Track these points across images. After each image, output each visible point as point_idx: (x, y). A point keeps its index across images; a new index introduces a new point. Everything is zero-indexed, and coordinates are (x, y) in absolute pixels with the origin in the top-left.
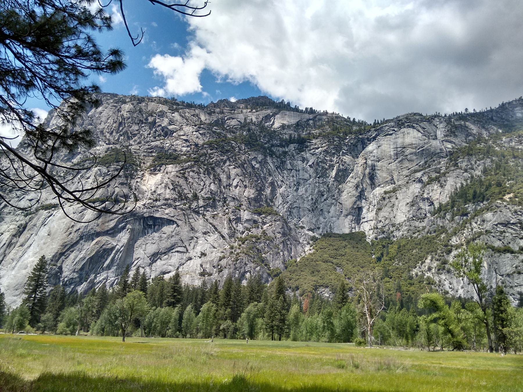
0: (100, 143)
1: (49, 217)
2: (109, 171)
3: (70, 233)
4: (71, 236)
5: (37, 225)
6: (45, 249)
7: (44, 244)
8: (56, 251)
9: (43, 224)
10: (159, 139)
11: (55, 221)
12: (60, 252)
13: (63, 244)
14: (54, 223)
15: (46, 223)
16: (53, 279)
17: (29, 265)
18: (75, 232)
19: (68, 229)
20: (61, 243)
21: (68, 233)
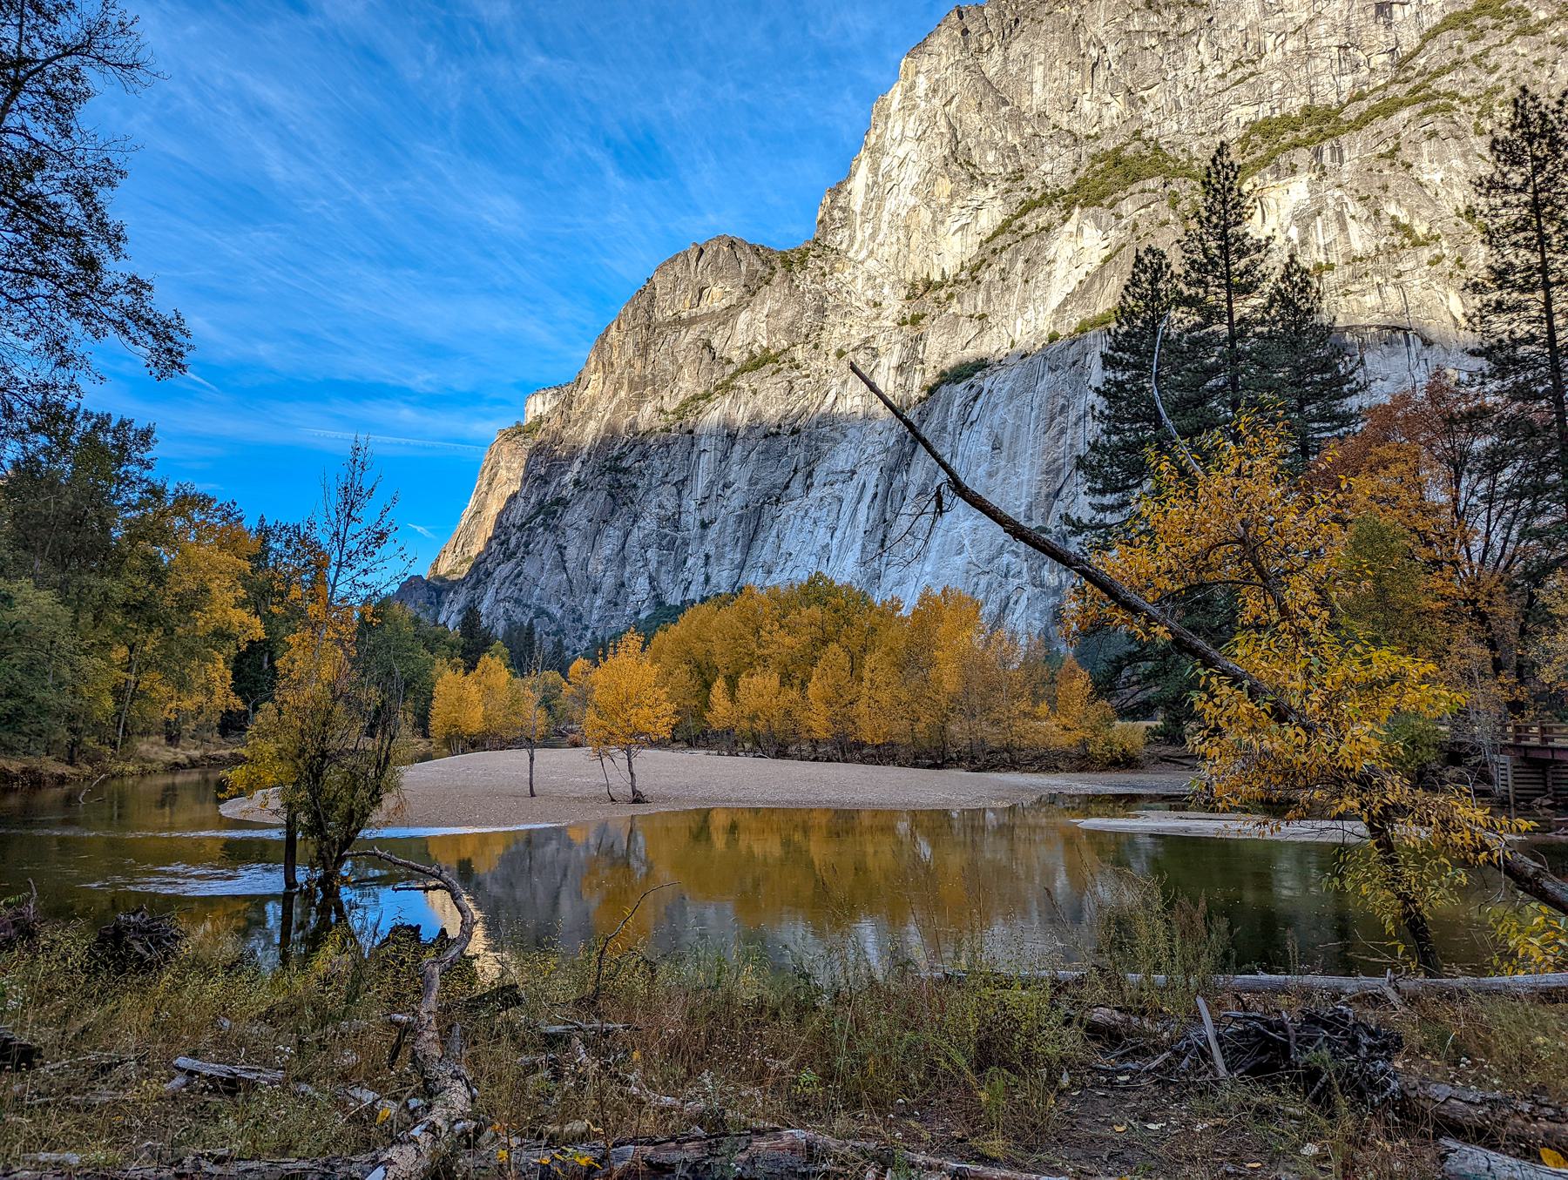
0: (1048, 149)
1: (975, 399)
2: (1119, 217)
3: (1062, 432)
4: (1067, 439)
5: (950, 428)
6: (999, 490)
7: (990, 475)
8: (1034, 491)
9: (965, 421)
10: (1238, 77)
11: (1000, 407)
12: (1044, 491)
13: (1049, 465)
14: (1000, 411)
15: (974, 416)
16: (1051, 572)
17: (966, 542)
18: (1076, 424)
19: (1052, 419)
20: (1041, 462)
21: (1053, 432)
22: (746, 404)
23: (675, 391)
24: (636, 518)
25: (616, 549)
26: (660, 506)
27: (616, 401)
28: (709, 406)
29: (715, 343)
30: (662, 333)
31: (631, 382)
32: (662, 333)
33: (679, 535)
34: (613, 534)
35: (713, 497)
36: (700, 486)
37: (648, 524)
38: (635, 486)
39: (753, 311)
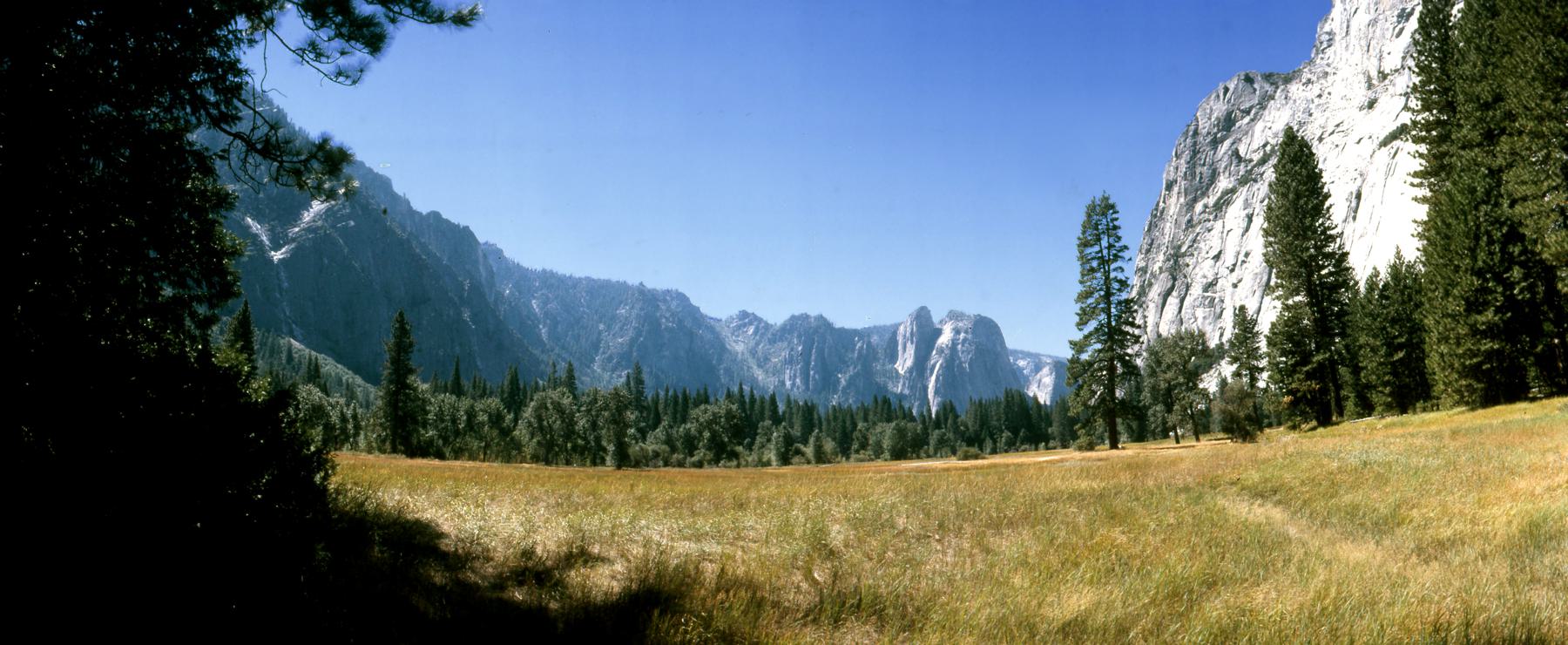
22: (1259, 189)
23: (1216, 190)
24: (1188, 287)
25: (1176, 313)
26: (1205, 277)
27: (1179, 205)
28: (1235, 197)
29: (1242, 153)
30: (1204, 151)
31: (1186, 190)
32: (1204, 151)
33: (1217, 295)
34: (1173, 301)
35: (1239, 263)
36: (1229, 259)
37: (1196, 290)
38: (1188, 265)
39: (1264, 120)
